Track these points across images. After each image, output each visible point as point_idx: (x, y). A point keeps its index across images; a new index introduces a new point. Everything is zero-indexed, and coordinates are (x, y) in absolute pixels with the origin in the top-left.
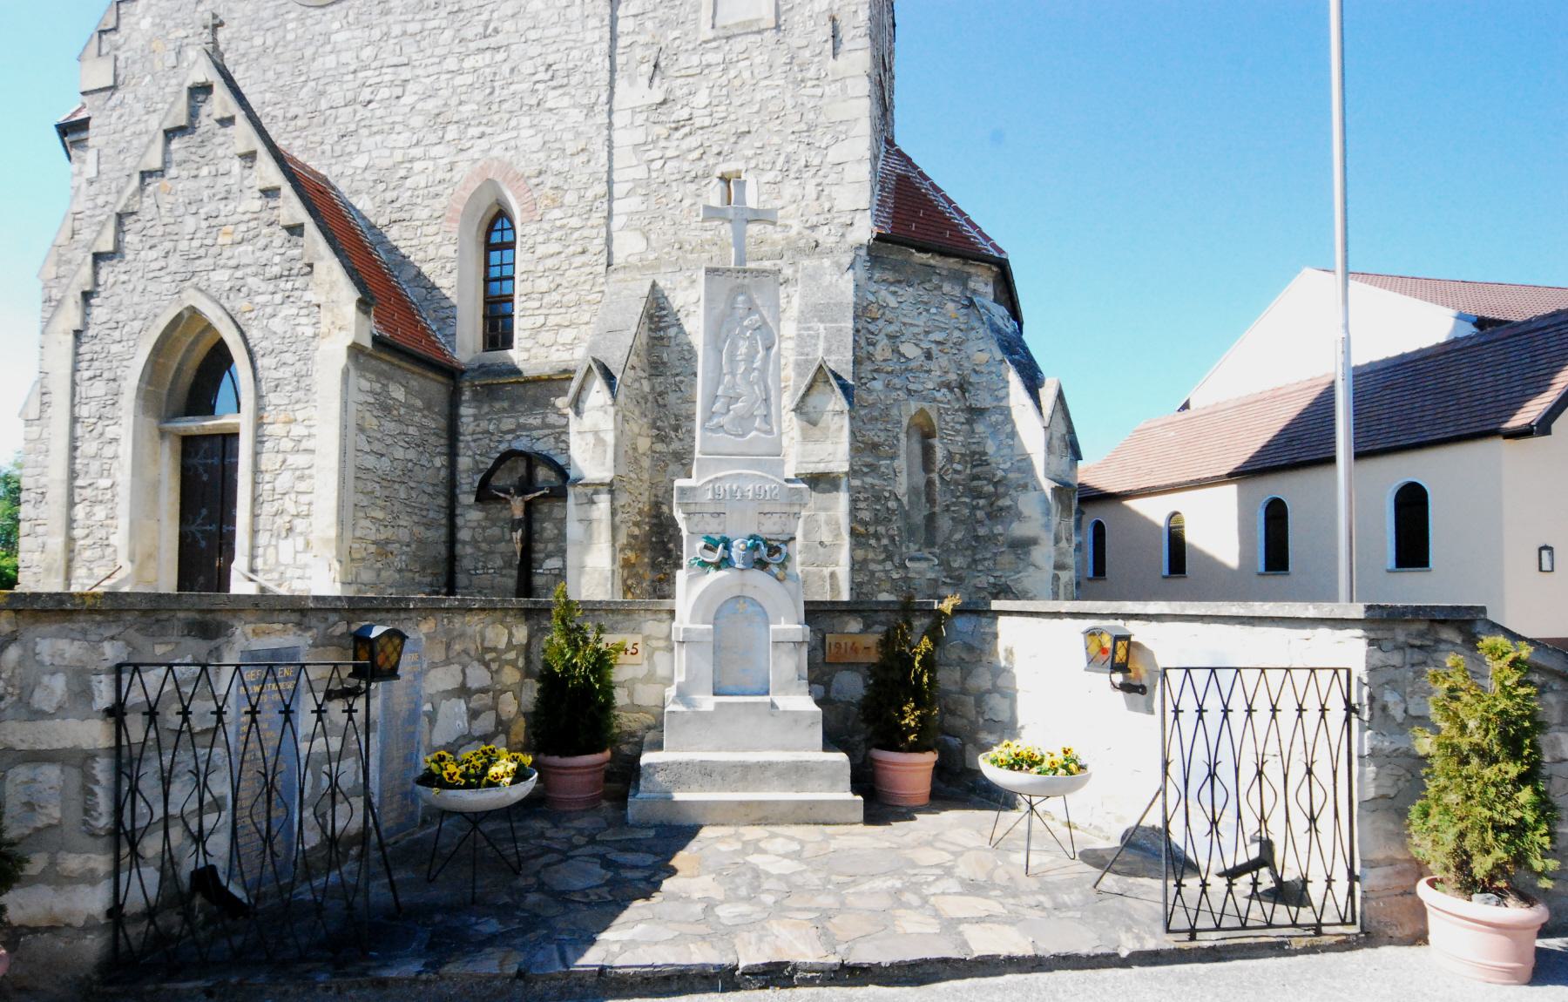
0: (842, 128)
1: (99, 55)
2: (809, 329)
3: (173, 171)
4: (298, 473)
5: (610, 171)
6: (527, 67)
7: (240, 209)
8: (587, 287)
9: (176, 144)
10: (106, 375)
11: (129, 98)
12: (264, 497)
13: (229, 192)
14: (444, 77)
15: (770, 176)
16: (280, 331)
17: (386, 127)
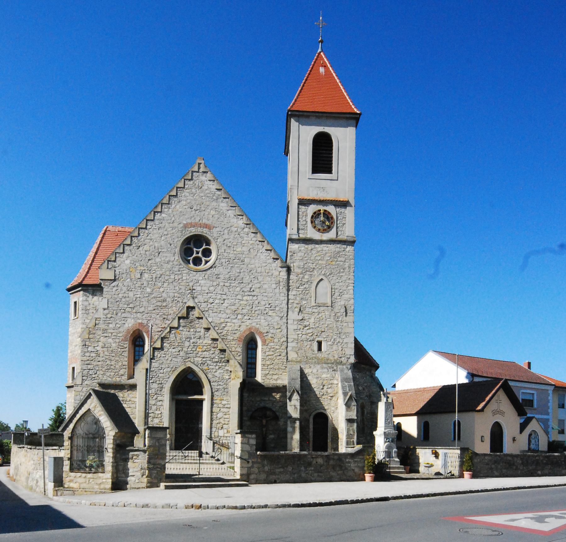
0: (347, 334)
1: (108, 268)
2: (344, 384)
3: (181, 328)
4: (224, 413)
5: (287, 335)
6: (263, 303)
7: (204, 342)
8: (281, 365)
9: (181, 321)
10: (158, 382)
11: (120, 284)
12: (214, 418)
13: (200, 337)
14: (237, 300)
15: (330, 343)
16: (218, 376)
17: (218, 311)
